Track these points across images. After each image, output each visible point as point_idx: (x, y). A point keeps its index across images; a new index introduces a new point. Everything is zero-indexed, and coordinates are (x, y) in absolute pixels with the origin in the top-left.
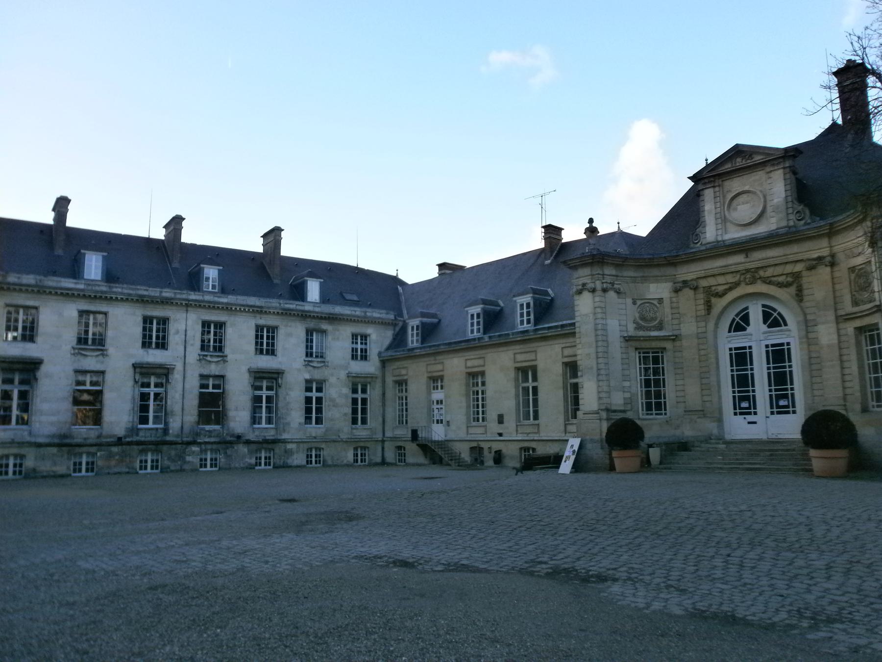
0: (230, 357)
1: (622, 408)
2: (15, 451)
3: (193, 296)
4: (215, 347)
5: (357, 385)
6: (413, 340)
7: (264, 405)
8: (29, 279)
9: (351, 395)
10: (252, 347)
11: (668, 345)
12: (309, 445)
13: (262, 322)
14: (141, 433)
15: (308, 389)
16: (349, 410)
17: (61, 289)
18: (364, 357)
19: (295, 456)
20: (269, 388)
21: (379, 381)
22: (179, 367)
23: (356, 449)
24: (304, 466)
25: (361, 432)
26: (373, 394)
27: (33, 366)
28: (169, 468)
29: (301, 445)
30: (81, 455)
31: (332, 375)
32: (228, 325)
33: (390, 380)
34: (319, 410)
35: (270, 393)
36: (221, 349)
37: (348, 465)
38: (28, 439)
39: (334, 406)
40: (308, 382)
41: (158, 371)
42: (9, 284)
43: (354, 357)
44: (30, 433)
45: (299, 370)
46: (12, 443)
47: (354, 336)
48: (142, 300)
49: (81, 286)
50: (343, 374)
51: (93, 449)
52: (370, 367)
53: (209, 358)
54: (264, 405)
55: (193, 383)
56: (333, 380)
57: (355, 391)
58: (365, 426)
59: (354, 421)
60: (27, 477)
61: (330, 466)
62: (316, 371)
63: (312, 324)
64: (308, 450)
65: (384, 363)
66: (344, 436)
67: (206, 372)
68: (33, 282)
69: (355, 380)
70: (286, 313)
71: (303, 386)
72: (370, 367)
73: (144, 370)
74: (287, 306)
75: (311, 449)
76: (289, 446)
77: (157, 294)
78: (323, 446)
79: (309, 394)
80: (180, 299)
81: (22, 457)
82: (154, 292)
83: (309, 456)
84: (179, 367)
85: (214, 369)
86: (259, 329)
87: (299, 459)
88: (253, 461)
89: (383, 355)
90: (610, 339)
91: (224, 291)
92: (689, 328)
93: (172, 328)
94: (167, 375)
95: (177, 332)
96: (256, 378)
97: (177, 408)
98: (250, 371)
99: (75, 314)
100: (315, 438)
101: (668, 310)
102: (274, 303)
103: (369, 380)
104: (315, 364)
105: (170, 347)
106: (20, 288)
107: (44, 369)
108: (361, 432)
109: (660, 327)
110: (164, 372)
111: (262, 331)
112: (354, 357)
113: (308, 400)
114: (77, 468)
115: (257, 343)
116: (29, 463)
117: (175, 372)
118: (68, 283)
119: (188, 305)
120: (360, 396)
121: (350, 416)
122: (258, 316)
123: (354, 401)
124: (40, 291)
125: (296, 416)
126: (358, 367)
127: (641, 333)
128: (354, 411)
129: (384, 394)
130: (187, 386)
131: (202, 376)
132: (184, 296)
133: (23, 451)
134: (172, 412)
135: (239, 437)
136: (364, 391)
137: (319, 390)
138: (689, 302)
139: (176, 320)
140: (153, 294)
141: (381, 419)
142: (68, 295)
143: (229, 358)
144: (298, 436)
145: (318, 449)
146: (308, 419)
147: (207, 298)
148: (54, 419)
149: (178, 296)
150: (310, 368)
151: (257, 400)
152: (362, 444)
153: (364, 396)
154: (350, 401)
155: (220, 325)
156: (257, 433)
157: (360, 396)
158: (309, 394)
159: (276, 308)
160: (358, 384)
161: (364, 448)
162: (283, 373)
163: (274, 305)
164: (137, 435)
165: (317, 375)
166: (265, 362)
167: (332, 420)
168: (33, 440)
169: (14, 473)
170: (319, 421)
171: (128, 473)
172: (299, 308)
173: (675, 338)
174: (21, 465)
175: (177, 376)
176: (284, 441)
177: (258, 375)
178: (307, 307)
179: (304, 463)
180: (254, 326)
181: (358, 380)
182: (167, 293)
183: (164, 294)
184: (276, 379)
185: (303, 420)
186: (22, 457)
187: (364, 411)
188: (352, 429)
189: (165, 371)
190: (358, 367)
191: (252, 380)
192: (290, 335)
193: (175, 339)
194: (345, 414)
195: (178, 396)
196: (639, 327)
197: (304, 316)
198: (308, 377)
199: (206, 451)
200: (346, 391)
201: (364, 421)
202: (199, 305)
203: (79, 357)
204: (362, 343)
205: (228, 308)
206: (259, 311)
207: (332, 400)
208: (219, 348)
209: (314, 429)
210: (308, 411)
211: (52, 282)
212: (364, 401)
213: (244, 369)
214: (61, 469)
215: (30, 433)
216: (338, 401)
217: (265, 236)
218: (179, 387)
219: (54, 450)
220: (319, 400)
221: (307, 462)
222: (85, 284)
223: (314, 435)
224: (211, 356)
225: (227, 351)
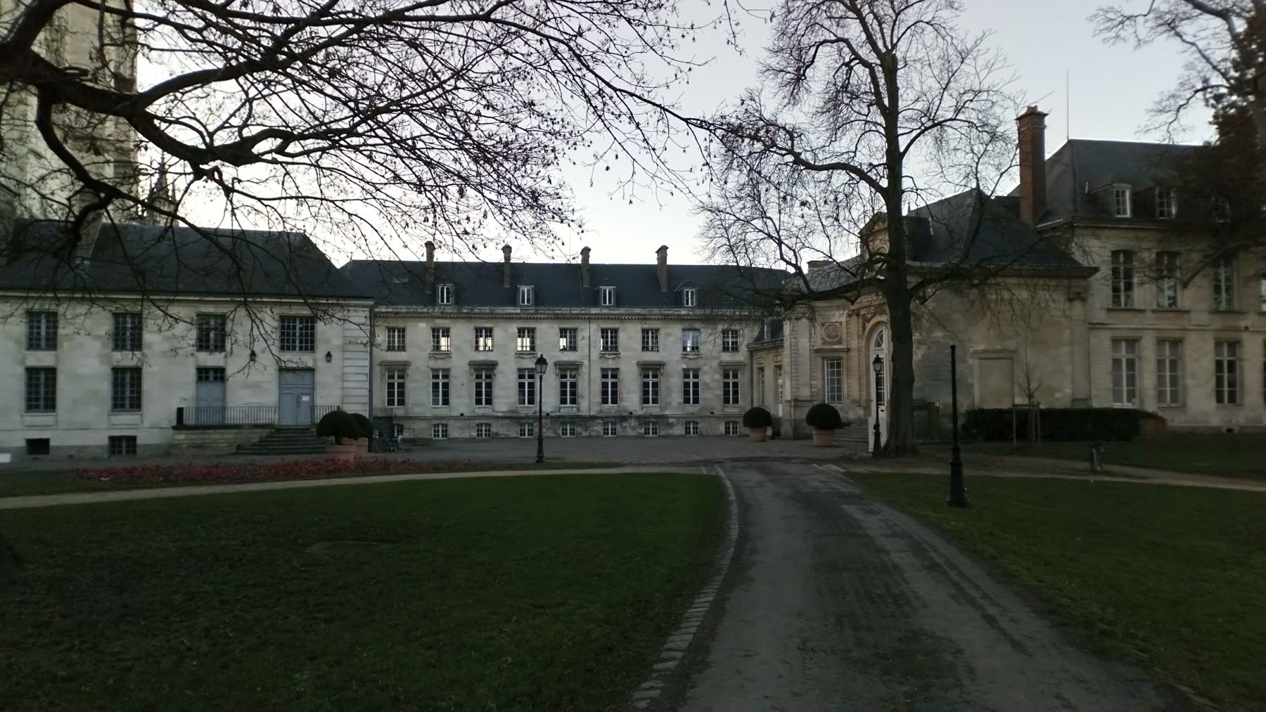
0: (623, 353)
1: (809, 399)
2: (484, 421)
3: (594, 311)
4: (612, 348)
5: (729, 371)
6: (766, 337)
7: (651, 389)
8: (486, 309)
9: (722, 380)
10: (640, 346)
11: (844, 355)
12: (688, 420)
13: (646, 326)
14: (562, 411)
15: (687, 376)
16: (720, 392)
17: (506, 314)
18: (735, 349)
19: (676, 428)
20: (655, 376)
21: (747, 370)
22: (586, 363)
23: (727, 423)
24: (683, 436)
25: (732, 410)
26: (743, 379)
27: (492, 367)
28: (581, 434)
29: (681, 420)
30: (524, 424)
31: (705, 364)
32: (620, 330)
33: (755, 366)
34: (696, 393)
35: (655, 380)
36: (616, 348)
37: (720, 436)
38: (492, 414)
39: (707, 389)
40: (684, 370)
41: (572, 367)
42: (475, 314)
43: (725, 349)
44: (493, 411)
45: (677, 362)
46: (484, 416)
47: (725, 332)
48: (557, 318)
49: (519, 311)
50: (715, 363)
51: (531, 421)
52: (741, 356)
53: (606, 356)
54: (651, 389)
55: (597, 374)
56: (706, 368)
57: (726, 376)
58: (737, 405)
59: (726, 401)
60: (493, 438)
61: (704, 436)
62: (691, 361)
63: (686, 325)
64: (686, 423)
65: (752, 352)
66: (717, 413)
67: (605, 366)
68: (488, 311)
69: (725, 368)
70: (666, 319)
71: (682, 374)
72: (741, 356)
73: (562, 367)
74: (667, 312)
75: (689, 423)
76: (671, 420)
77: (568, 312)
78: (698, 420)
79: (687, 380)
80: (583, 314)
81: (490, 425)
82: (566, 310)
83: (687, 429)
84: (586, 363)
85: (611, 364)
86: (645, 332)
87: (679, 430)
88: (642, 431)
89: (750, 346)
90: (800, 352)
91: (619, 303)
92: (854, 344)
93: (580, 335)
94: (577, 369)
95: (583, 338)
96: (643, 369)
97: (586, 394)
98: (639, 364)
99: (516, 331)
100: (692, 414)
101: (844, 330)
102: (656, 311)
103: (738, 367)
104: (690, 357)
105: (579, 350)
106: (481, 316)
107: (499, 368)
108: (732, 410)
109: (840, 342)
110: (575, 367)
111: (648, 333)
112: (725, 349)
113: (686, 385)
114: (522, 431)
115: (643, 342)
116: (494, 429)
117: (583, 367)
118: (510, 310)
119: (590, 319)
120: (731, 381)
121: (722, 398)
122: (643, 322)
123: (726, 385)
124: (493, 317)
125: (677, 397)
126: (727, 357)
127: (828, 347)
128: (726, 393)
129: (752, 379)
130: (592, 377)
131: (603, 370)
132: (587, 312)
133: (489, 422)
134: (582, 395)
135: (631, 413)
136: (735, 376)
137: (696, 376)
138: (855, 324)
139: (582, 330)
140: (565, 312)
141: (749, 399)
142: (510, 318)
143: (621, 356)
144: (678, 412)
145: (697, 423)
146: (687, 401)
147: (605, 311)
148: (506, 400)
149: (583, 312)
150: (687, 360)
151: (646, 385)
152: (732, 419)
153: (735, 380)
154: (722, 384)
155: (615, 331)
156: (645, 410)
157: (731, 381)
158: (687, 380)
159: (656, 315)
160: (729, 371)
161: (734, 423)
162: (664, 365)
163: (655, 312)
164: (559, 411)
165: (693, 365)
166: (650, 357)
167: (705, 400)
168: (495, 414)
169: (486, 435)
170: (696, 401)
171: (554, 437)
172: (676, 313)
173: (848, 350)
174: (489, 430)
175: (584, 370)
176: (666, 417)
177: (644, 367)
178: (683, 312)
179: (683, 433)
180: (640, 330)
181: (728, 368)
182: (576, 311)
183: (573, 312)
184: (659, 369)
185: (682, 400)
186: (490, 425)
187: (736, 393)
188: (724, 407)
189: (576, 367)
190: (727, 357)
191: (640, 370)
192: (669, 335)
193: (582, 343)
194: (717, 396)
195: (586, 384)
196: (825, 343)
197: (680, 319)
198: (684, 366)
199: (607, 423)
200: (718, 377)
201: (736, 401)
202: (599, 318)
203: (520, 359)
204: (732, 337)
205: (619, 318)
206: (644, 318)
207: (706, 384)
208: (615, 348)
209: (691, 408)
210: (686, 393)
211: (499, 310)
212: (735, 385)
213: (634, 362)
214: (514, 435)
215: (493, 411)
216: (711, 385)
217: (658, 252)
218: (586, 377)
219: (507, 421)
220: (696, 385)
221: (686, 433)
222: (521, 310)
223: (691, 411)
224: (609, 354)
225: (620, 350)
